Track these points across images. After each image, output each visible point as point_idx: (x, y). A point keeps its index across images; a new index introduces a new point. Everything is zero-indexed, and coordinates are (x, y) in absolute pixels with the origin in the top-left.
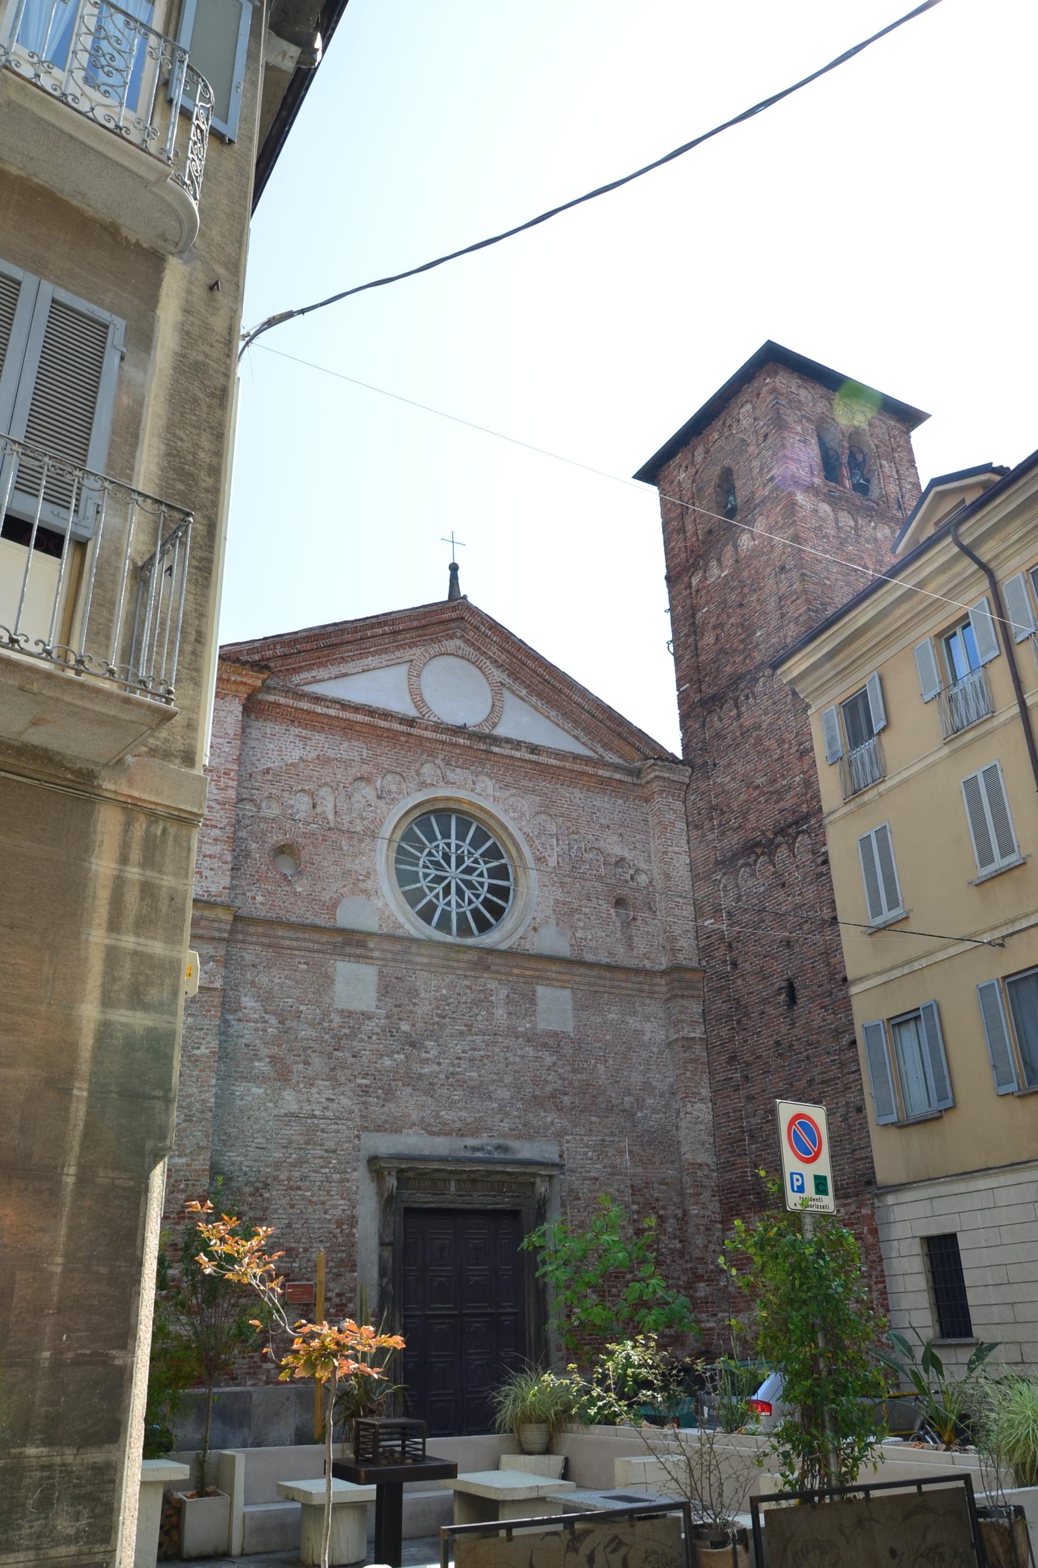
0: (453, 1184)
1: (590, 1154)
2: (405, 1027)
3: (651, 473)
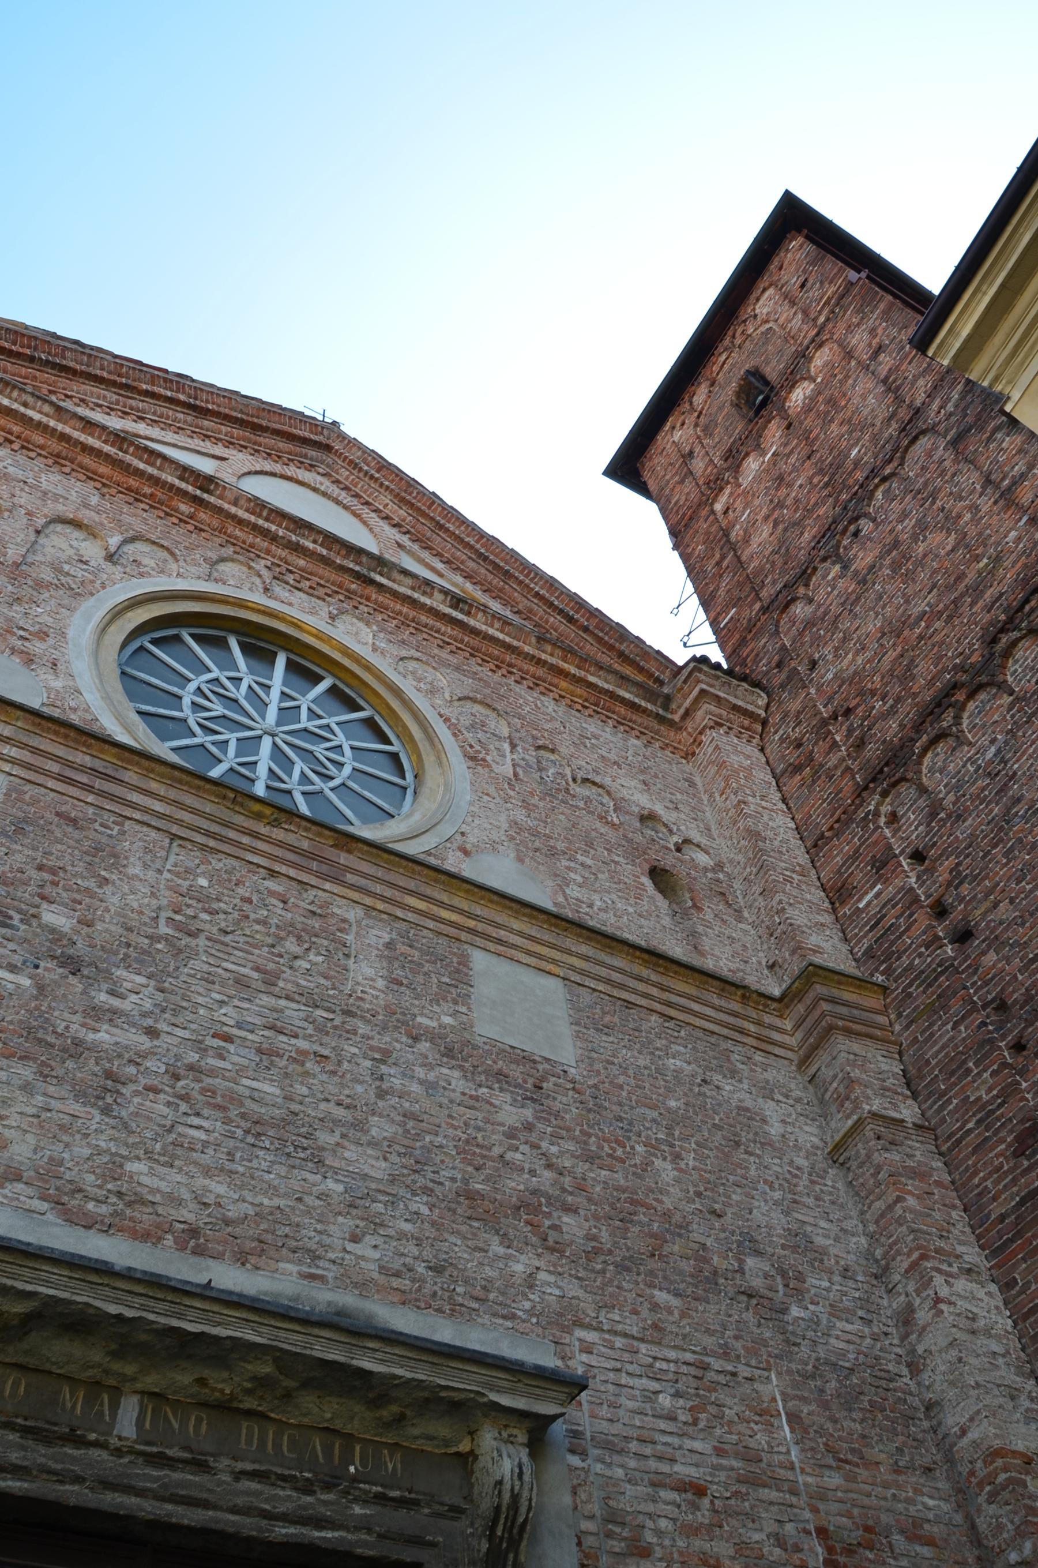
0: (129, 1410)
1: (665, 1401)
2: (54, 917)
3: (628, 467)
